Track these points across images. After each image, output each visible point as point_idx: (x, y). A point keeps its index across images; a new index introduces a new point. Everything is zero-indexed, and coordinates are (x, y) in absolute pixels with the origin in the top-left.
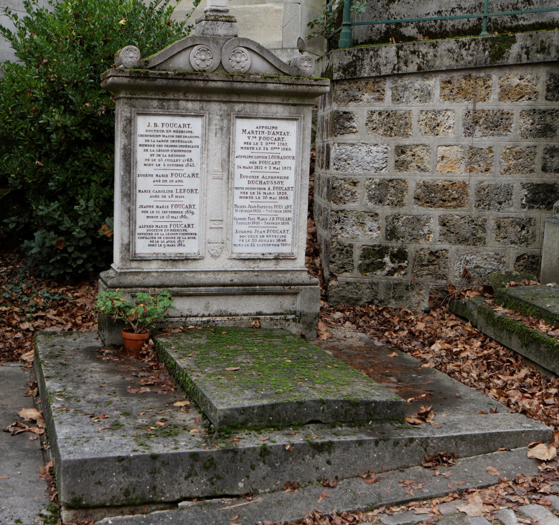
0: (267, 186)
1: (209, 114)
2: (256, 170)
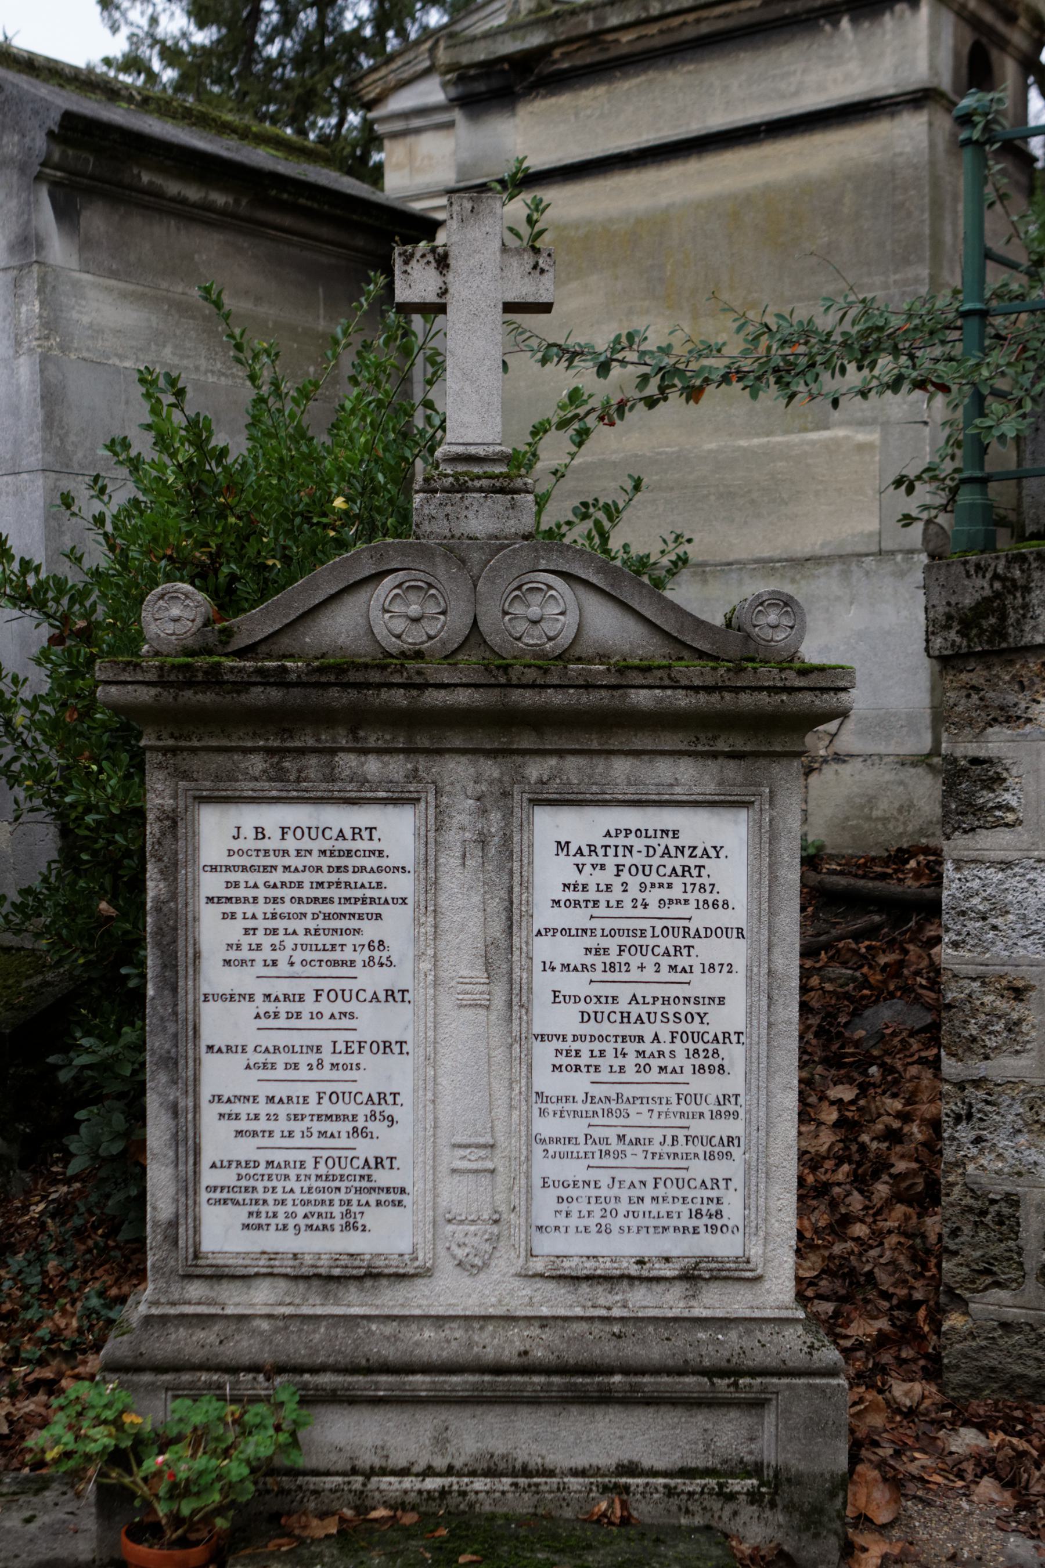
0: (647, 1031)
1: (438, 793)
2: (609, 976)
